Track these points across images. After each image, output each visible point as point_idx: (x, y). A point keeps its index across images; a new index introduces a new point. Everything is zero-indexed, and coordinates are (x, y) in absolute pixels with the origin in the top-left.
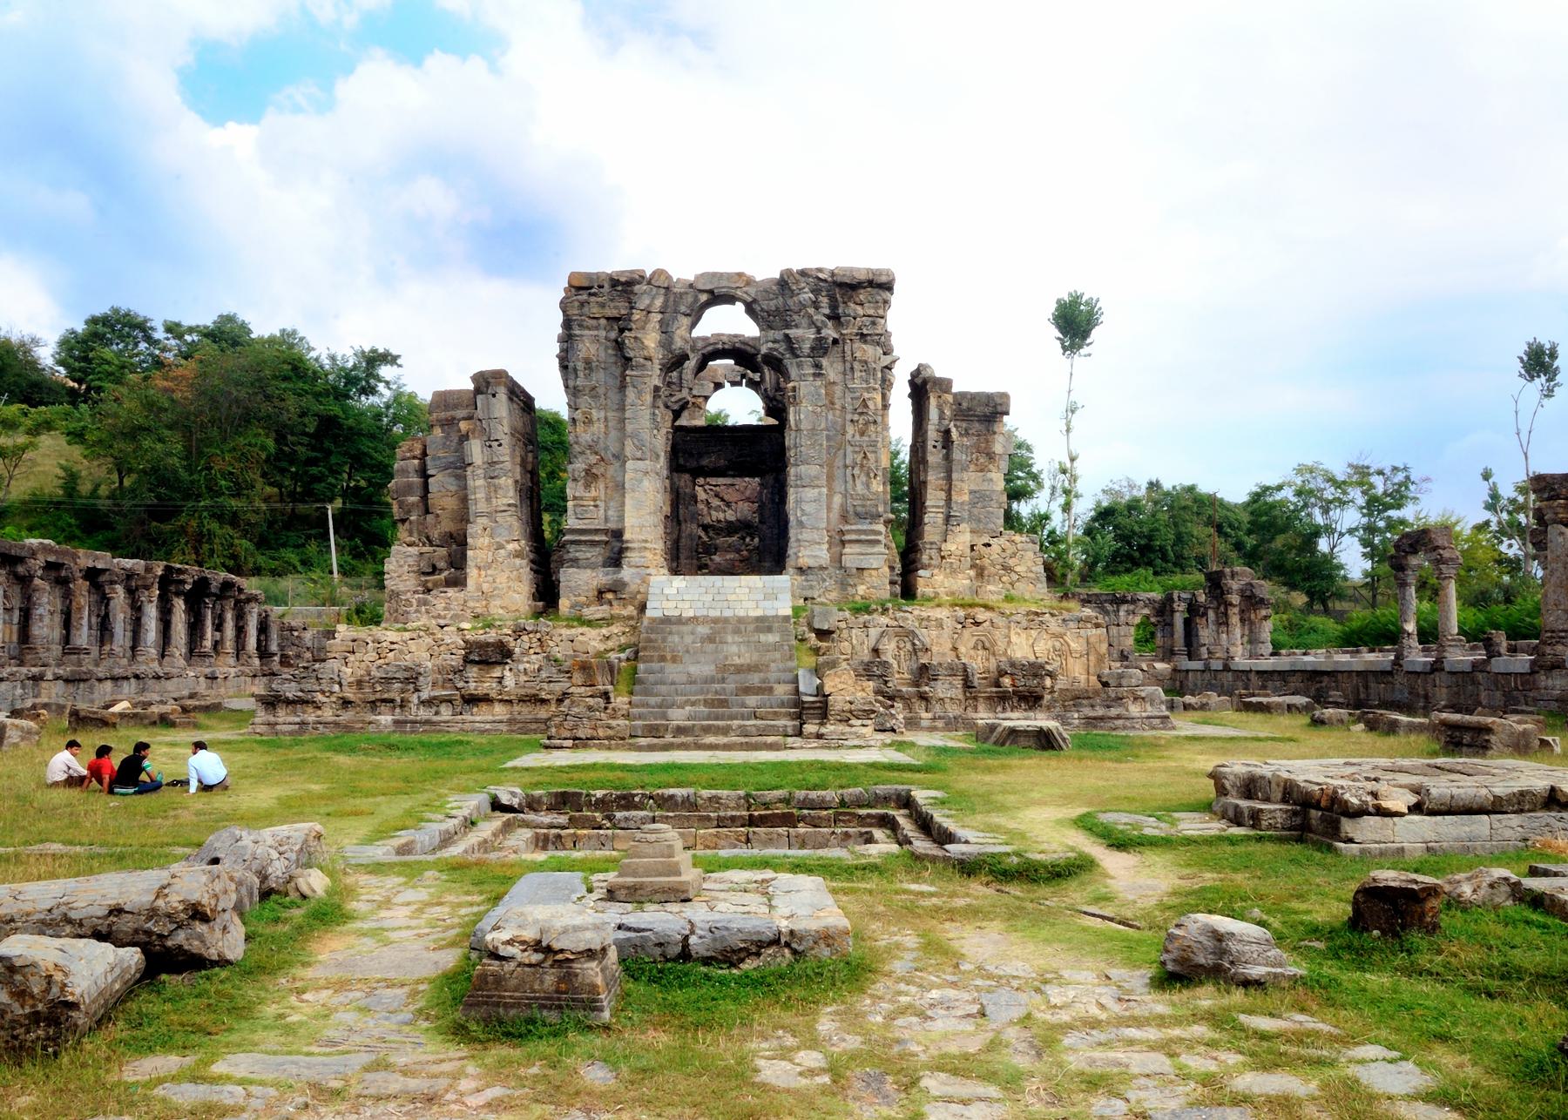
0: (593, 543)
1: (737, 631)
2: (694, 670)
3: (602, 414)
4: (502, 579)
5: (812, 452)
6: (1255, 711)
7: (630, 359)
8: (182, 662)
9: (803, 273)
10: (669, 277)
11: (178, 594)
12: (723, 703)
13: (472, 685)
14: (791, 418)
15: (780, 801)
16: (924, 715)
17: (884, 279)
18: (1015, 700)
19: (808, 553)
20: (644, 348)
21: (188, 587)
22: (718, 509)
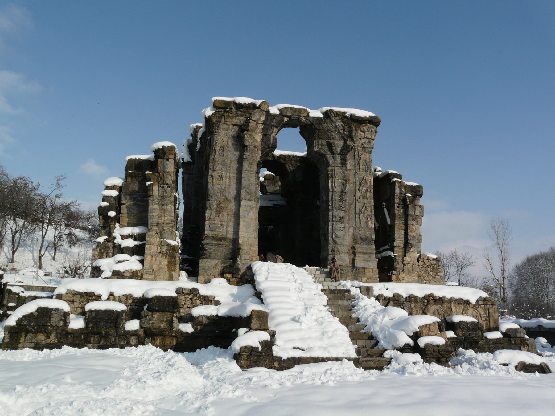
7: (246, 146)
17: (376, 121)
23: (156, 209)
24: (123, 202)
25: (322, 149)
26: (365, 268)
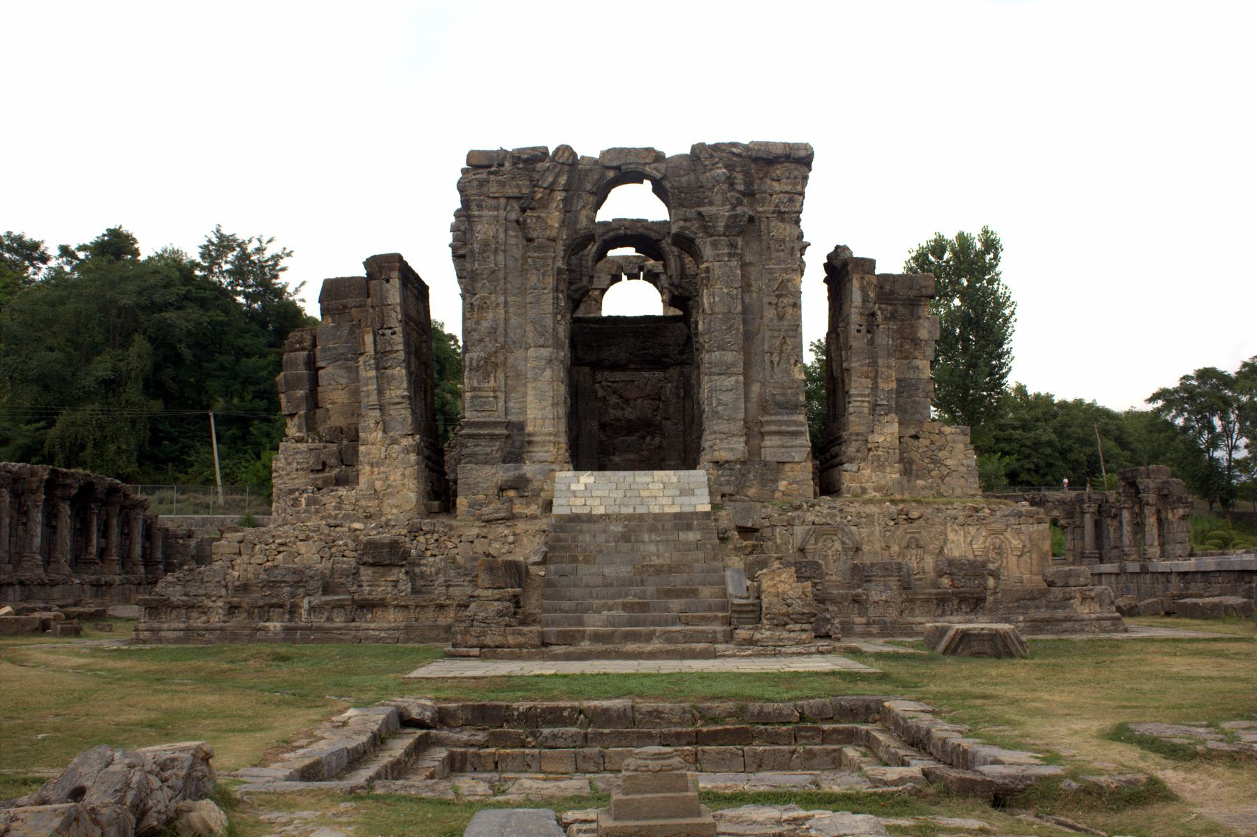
0: (493, 437)
1: (652, 529)
2: (608, 571)
3: (502, 299)
4: (395, 477)
5: (728, 338)
6: (1192, 617)
8: (68, 569)
9: (717, 147)
10: (574, 154)
11: (63, 499)
12: (644, 607)
13: (366, 589)
14: (705, 301)
15: (730, 715)
16: (858, 620)
17: (802, 153)
18: (956, 602)
19: (724, 445)
21: (74, 492)
22: (616, 406)
23: (370, 378)
24: (320, 364)
25: (688, 228)
26: (784, 463)
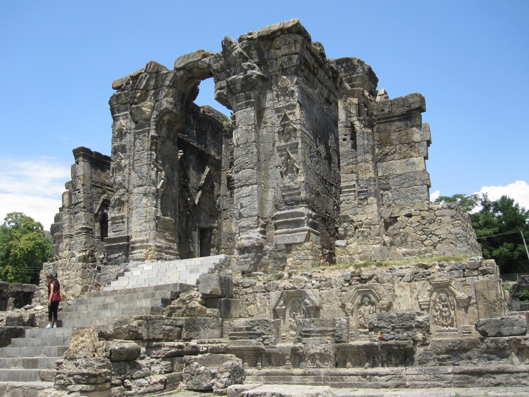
5: (246, 159)
19: (244, 236)
20: (143, 113)
